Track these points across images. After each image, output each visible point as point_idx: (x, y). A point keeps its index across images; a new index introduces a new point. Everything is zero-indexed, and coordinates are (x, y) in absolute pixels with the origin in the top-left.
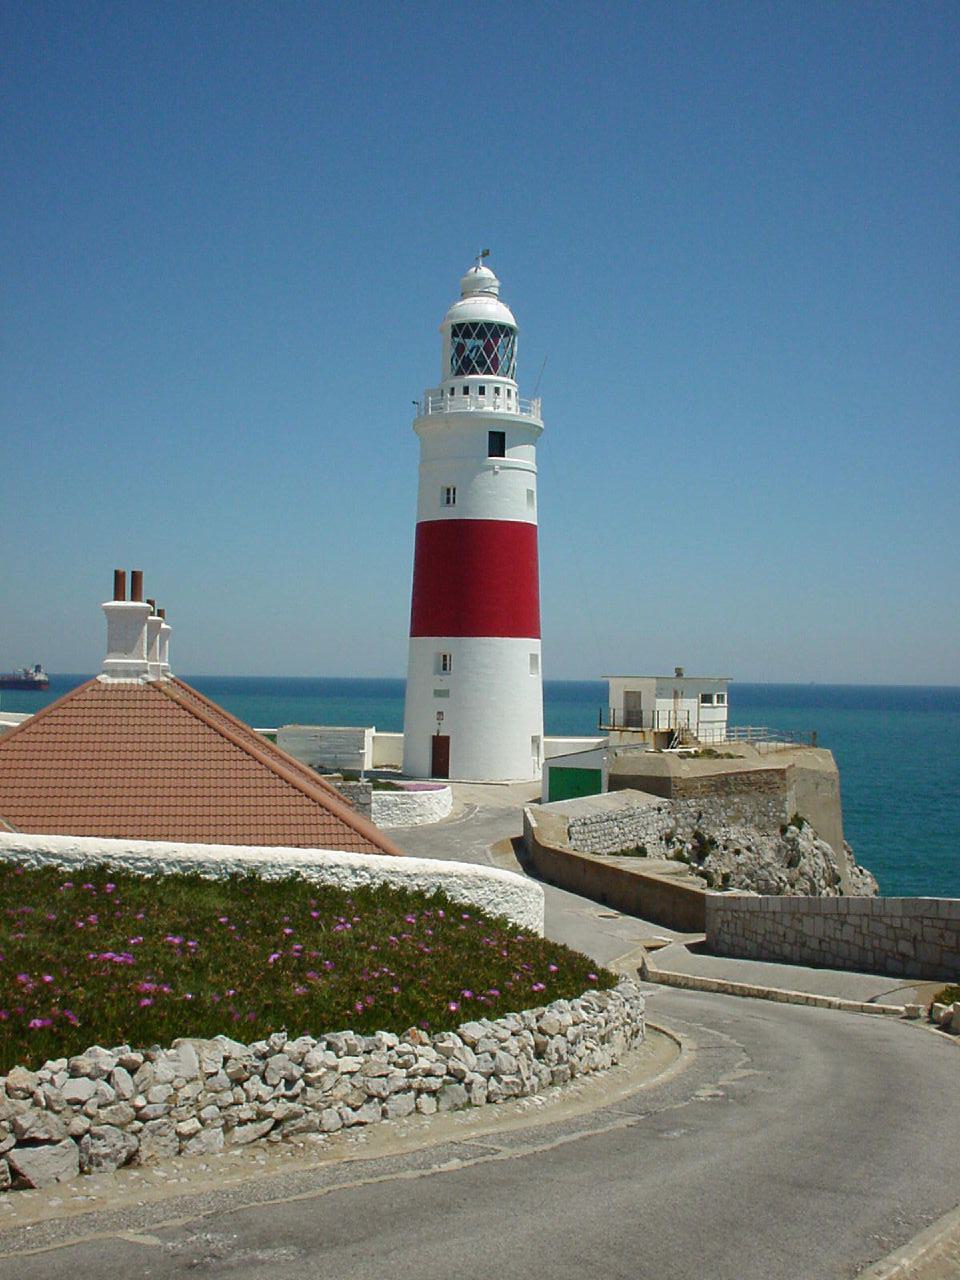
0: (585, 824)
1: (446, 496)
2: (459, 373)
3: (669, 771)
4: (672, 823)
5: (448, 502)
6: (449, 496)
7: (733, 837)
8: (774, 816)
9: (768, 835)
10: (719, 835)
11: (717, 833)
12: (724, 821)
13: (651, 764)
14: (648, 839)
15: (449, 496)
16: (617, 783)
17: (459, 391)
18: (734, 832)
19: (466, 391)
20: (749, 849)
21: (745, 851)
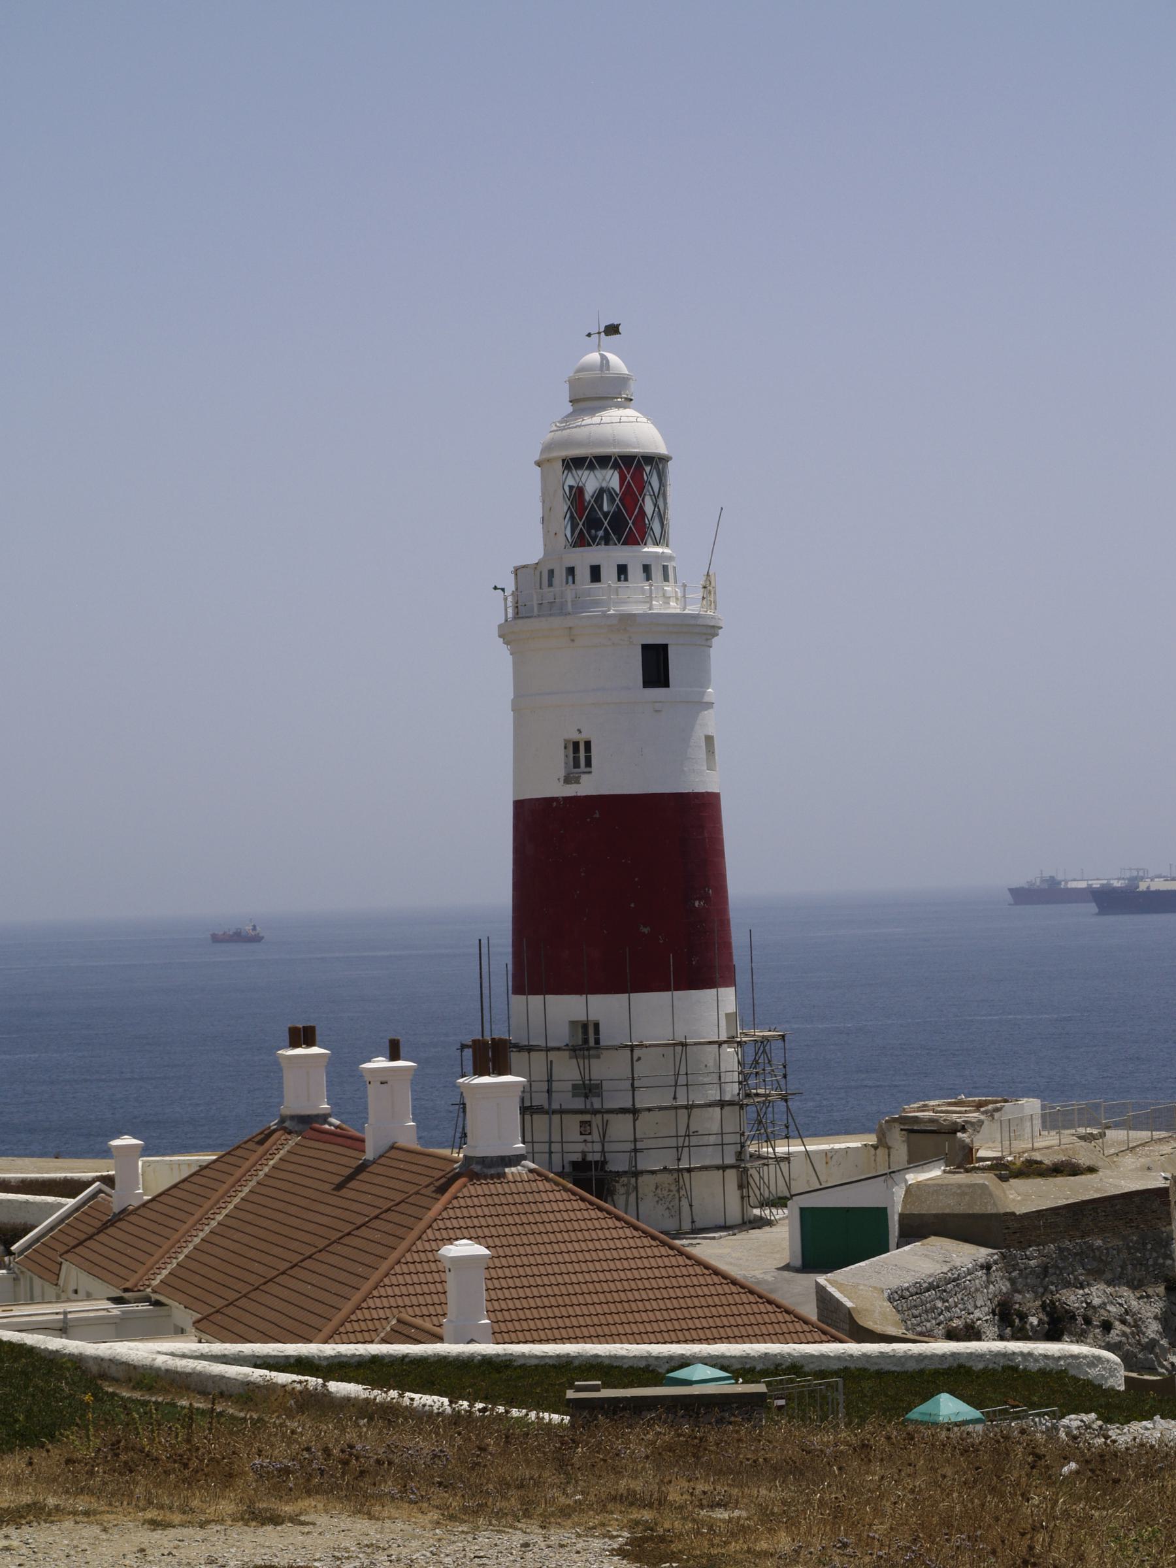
0: (903, 1297)
1: (571, 756)
2: (580, 541)
3: (995, 1204)
4: (1005, 1287)
5: (576, 764)
6: (580, 754)
7: (1096, 1302)
8: (1155, 1263)
9: (1148, 1297)
10: (1072, 1299)
11: (1073, 1298)
12: (1082, 1278)
13: (964, 1194)
14: (977, 1314)
15: (580, 754)
16: (916, 1229)
17: (583, 574)
18: (1097, 1293)
19: (596, 574)
20: (1123, 1322)
21: (1117, 1323)
